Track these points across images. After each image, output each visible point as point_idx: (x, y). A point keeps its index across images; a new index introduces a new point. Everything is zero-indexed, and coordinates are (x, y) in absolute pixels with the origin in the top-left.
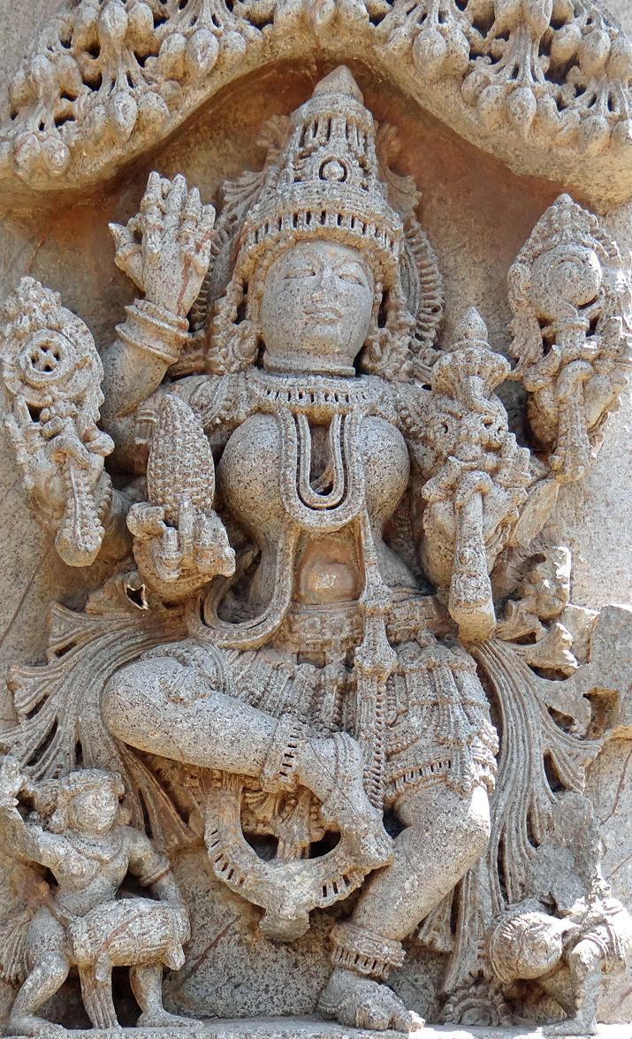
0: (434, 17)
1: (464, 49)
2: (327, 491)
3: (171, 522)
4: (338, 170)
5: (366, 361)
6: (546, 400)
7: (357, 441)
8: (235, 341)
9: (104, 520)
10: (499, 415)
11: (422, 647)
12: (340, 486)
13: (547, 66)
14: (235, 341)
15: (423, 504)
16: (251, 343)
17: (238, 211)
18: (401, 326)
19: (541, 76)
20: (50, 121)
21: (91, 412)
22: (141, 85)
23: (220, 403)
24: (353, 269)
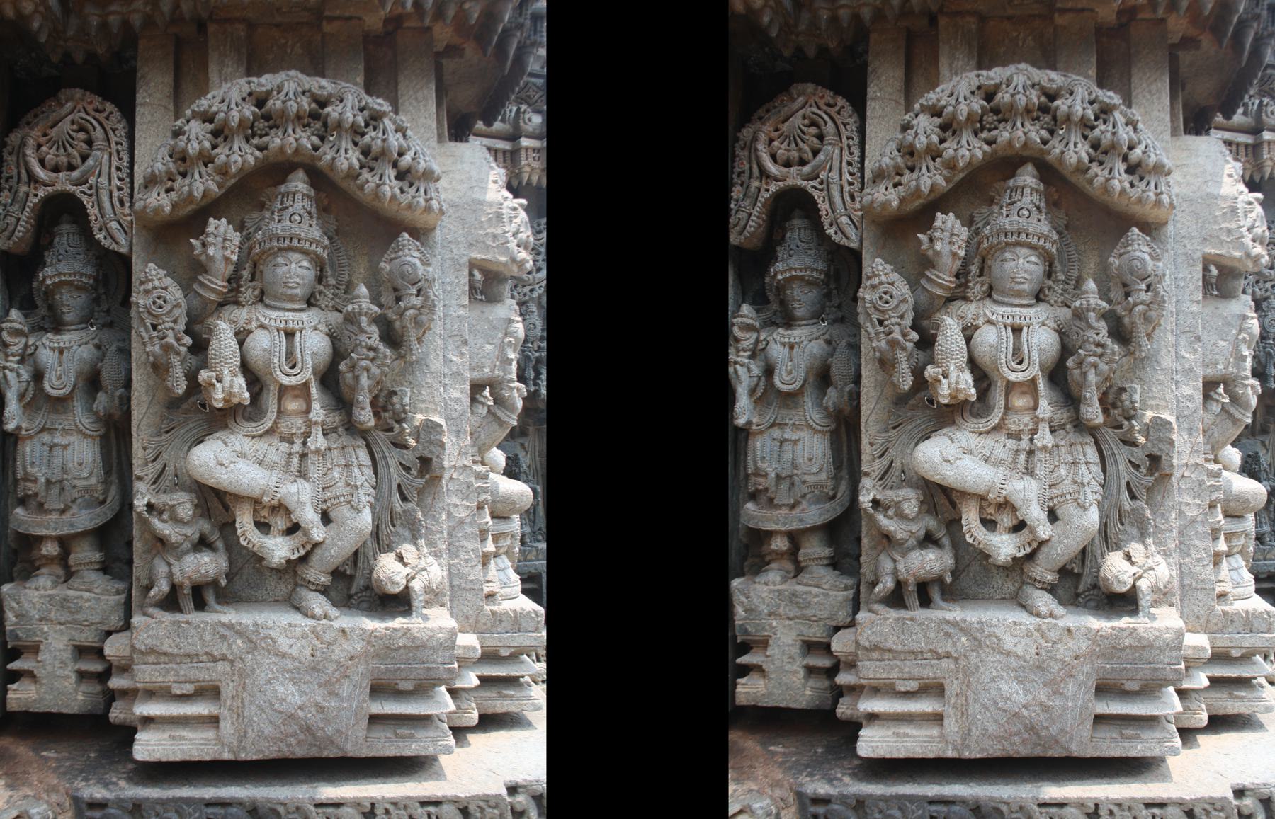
0: (1071, 145)
1: (1086, 158)
2: (1020, 363)
3: (946, 377)
4: (1026, 213)
5: (1041, 296)
6: (1126, 320)
7: (1035, 340)
8: (978, 286)
9: (913, 372)
10: (1103, 327)
11: (1068, 433)
12: (1026, 361)
13: (1125, 167)
14: (978, 286)
15: (1066, 368)
16: (985, 288)
17: (980, 225)
18: (1058, 281)
19: (1122, 171)
20: (890, 186)
21: (908, 322)
22: (934, 171)
23: (970, 316)
24: (1033, 259)
